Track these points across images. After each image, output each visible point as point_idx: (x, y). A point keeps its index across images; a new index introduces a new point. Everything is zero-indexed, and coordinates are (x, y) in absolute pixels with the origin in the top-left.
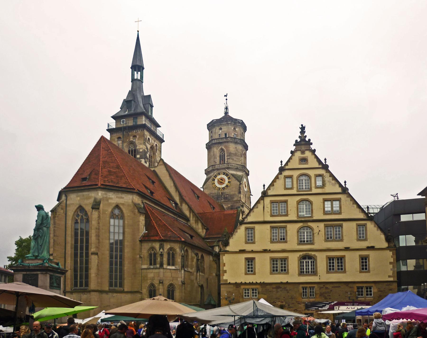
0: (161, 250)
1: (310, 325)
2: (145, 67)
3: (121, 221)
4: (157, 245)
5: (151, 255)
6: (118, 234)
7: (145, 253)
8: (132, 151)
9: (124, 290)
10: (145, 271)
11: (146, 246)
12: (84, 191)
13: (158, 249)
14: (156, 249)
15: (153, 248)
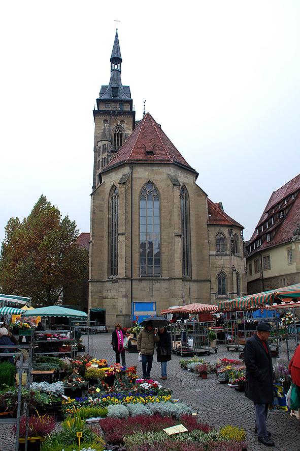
0: (232, 236)
1: (290, 313)
2: (122, 58)
3: (157, 204)
4: (225, 231)
5: (218, 241)
6: (148, 215)
7: (212, 238)
8: (118, 135)
9: (191, 278)
10: (213, 257)
11: (214, 231)
12: (153, 166)
13: (227, 235)
14: (223, 235)
15: (220, 233)
